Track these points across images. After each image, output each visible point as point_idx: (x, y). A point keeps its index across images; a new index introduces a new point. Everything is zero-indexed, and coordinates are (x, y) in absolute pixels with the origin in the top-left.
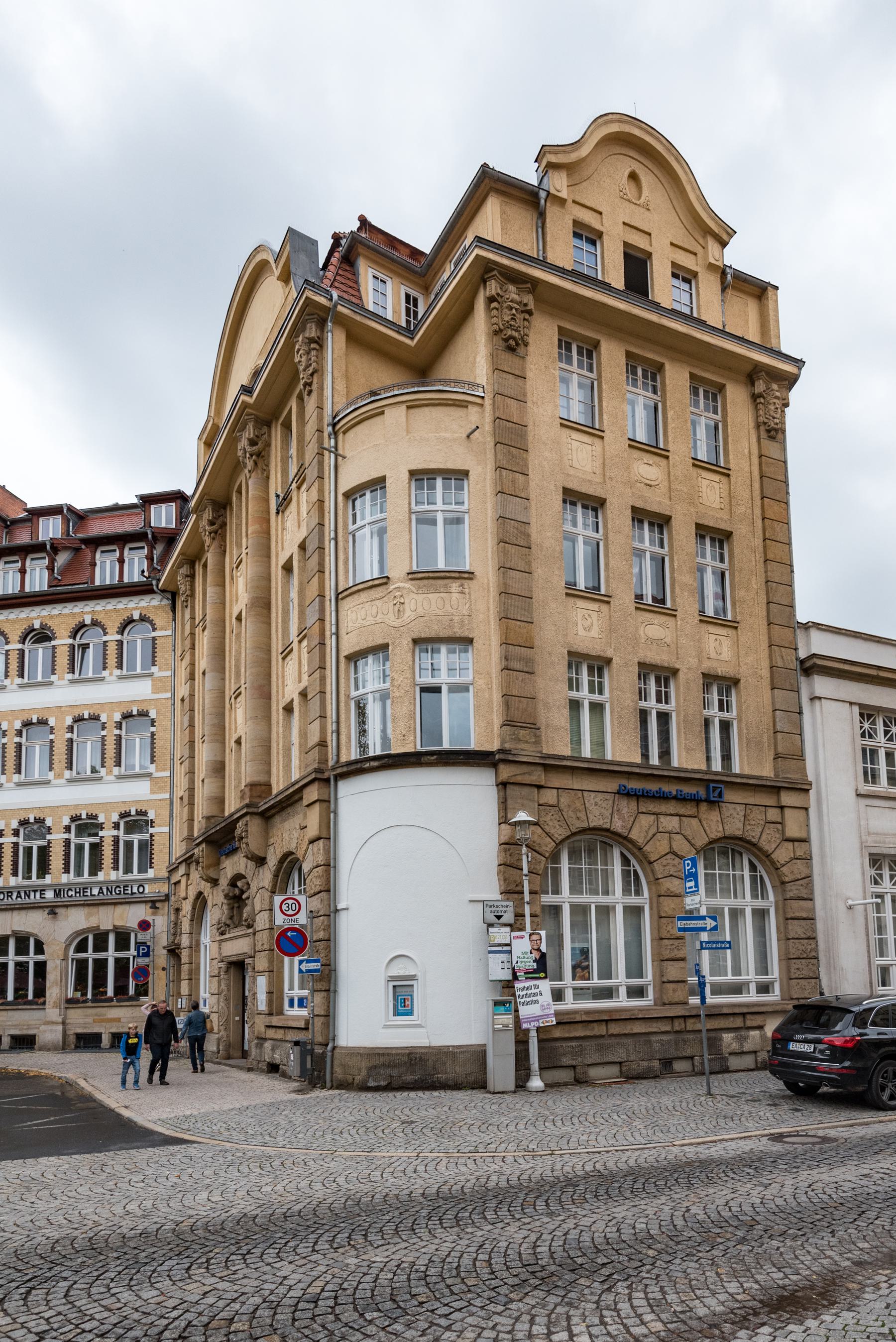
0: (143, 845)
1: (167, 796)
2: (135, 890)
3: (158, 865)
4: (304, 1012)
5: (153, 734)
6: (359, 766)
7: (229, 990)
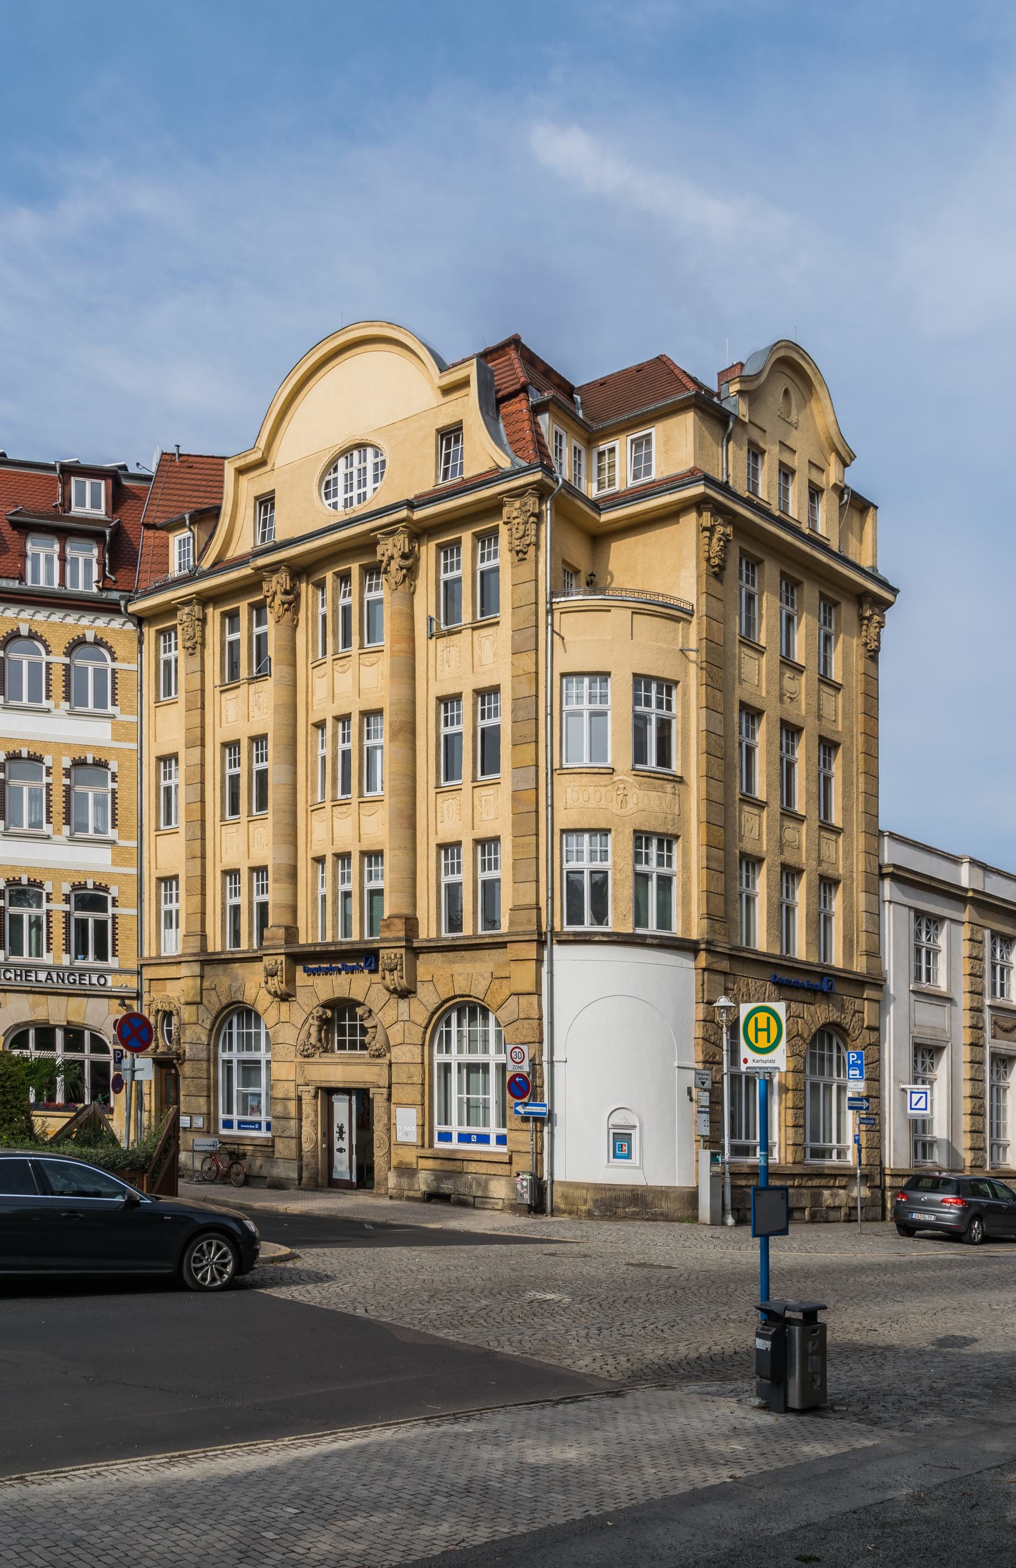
0: (101, 927)
1: (134, 871)
2: (94, 980)
3: (124, 953)
4: (503, 1149)
5: (114, 792)
6: (587, 938)
7: (316, 1116)
